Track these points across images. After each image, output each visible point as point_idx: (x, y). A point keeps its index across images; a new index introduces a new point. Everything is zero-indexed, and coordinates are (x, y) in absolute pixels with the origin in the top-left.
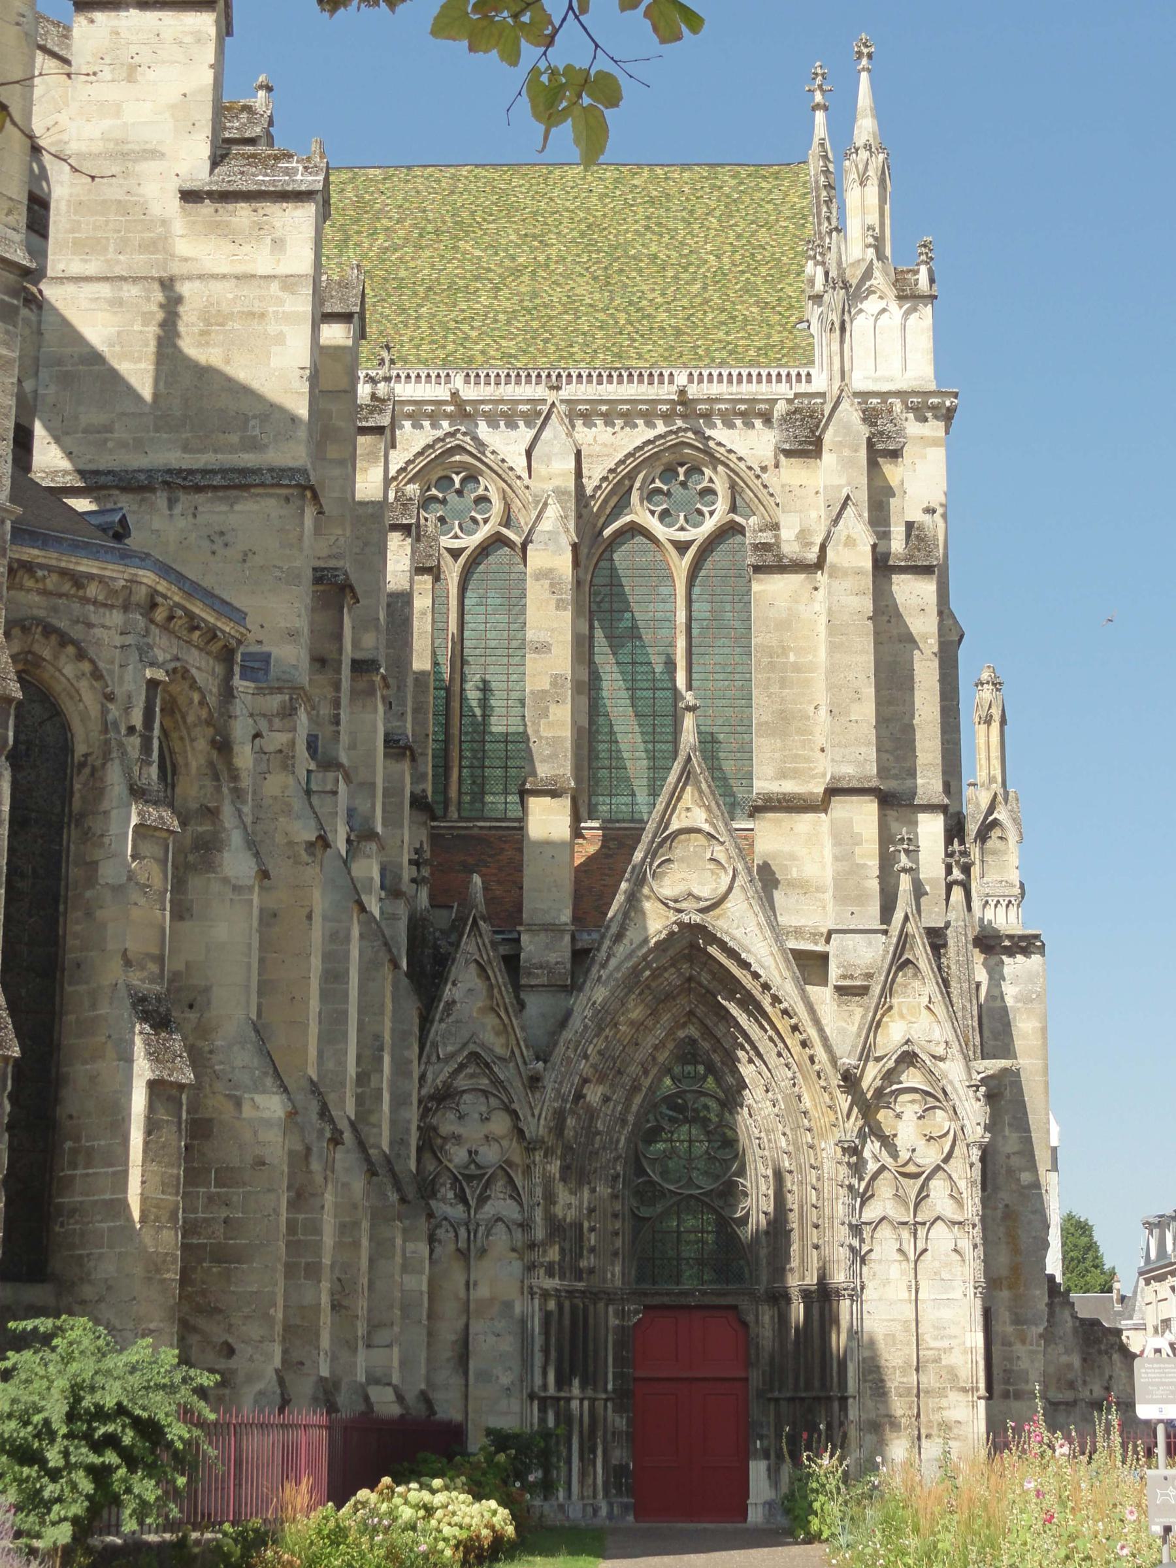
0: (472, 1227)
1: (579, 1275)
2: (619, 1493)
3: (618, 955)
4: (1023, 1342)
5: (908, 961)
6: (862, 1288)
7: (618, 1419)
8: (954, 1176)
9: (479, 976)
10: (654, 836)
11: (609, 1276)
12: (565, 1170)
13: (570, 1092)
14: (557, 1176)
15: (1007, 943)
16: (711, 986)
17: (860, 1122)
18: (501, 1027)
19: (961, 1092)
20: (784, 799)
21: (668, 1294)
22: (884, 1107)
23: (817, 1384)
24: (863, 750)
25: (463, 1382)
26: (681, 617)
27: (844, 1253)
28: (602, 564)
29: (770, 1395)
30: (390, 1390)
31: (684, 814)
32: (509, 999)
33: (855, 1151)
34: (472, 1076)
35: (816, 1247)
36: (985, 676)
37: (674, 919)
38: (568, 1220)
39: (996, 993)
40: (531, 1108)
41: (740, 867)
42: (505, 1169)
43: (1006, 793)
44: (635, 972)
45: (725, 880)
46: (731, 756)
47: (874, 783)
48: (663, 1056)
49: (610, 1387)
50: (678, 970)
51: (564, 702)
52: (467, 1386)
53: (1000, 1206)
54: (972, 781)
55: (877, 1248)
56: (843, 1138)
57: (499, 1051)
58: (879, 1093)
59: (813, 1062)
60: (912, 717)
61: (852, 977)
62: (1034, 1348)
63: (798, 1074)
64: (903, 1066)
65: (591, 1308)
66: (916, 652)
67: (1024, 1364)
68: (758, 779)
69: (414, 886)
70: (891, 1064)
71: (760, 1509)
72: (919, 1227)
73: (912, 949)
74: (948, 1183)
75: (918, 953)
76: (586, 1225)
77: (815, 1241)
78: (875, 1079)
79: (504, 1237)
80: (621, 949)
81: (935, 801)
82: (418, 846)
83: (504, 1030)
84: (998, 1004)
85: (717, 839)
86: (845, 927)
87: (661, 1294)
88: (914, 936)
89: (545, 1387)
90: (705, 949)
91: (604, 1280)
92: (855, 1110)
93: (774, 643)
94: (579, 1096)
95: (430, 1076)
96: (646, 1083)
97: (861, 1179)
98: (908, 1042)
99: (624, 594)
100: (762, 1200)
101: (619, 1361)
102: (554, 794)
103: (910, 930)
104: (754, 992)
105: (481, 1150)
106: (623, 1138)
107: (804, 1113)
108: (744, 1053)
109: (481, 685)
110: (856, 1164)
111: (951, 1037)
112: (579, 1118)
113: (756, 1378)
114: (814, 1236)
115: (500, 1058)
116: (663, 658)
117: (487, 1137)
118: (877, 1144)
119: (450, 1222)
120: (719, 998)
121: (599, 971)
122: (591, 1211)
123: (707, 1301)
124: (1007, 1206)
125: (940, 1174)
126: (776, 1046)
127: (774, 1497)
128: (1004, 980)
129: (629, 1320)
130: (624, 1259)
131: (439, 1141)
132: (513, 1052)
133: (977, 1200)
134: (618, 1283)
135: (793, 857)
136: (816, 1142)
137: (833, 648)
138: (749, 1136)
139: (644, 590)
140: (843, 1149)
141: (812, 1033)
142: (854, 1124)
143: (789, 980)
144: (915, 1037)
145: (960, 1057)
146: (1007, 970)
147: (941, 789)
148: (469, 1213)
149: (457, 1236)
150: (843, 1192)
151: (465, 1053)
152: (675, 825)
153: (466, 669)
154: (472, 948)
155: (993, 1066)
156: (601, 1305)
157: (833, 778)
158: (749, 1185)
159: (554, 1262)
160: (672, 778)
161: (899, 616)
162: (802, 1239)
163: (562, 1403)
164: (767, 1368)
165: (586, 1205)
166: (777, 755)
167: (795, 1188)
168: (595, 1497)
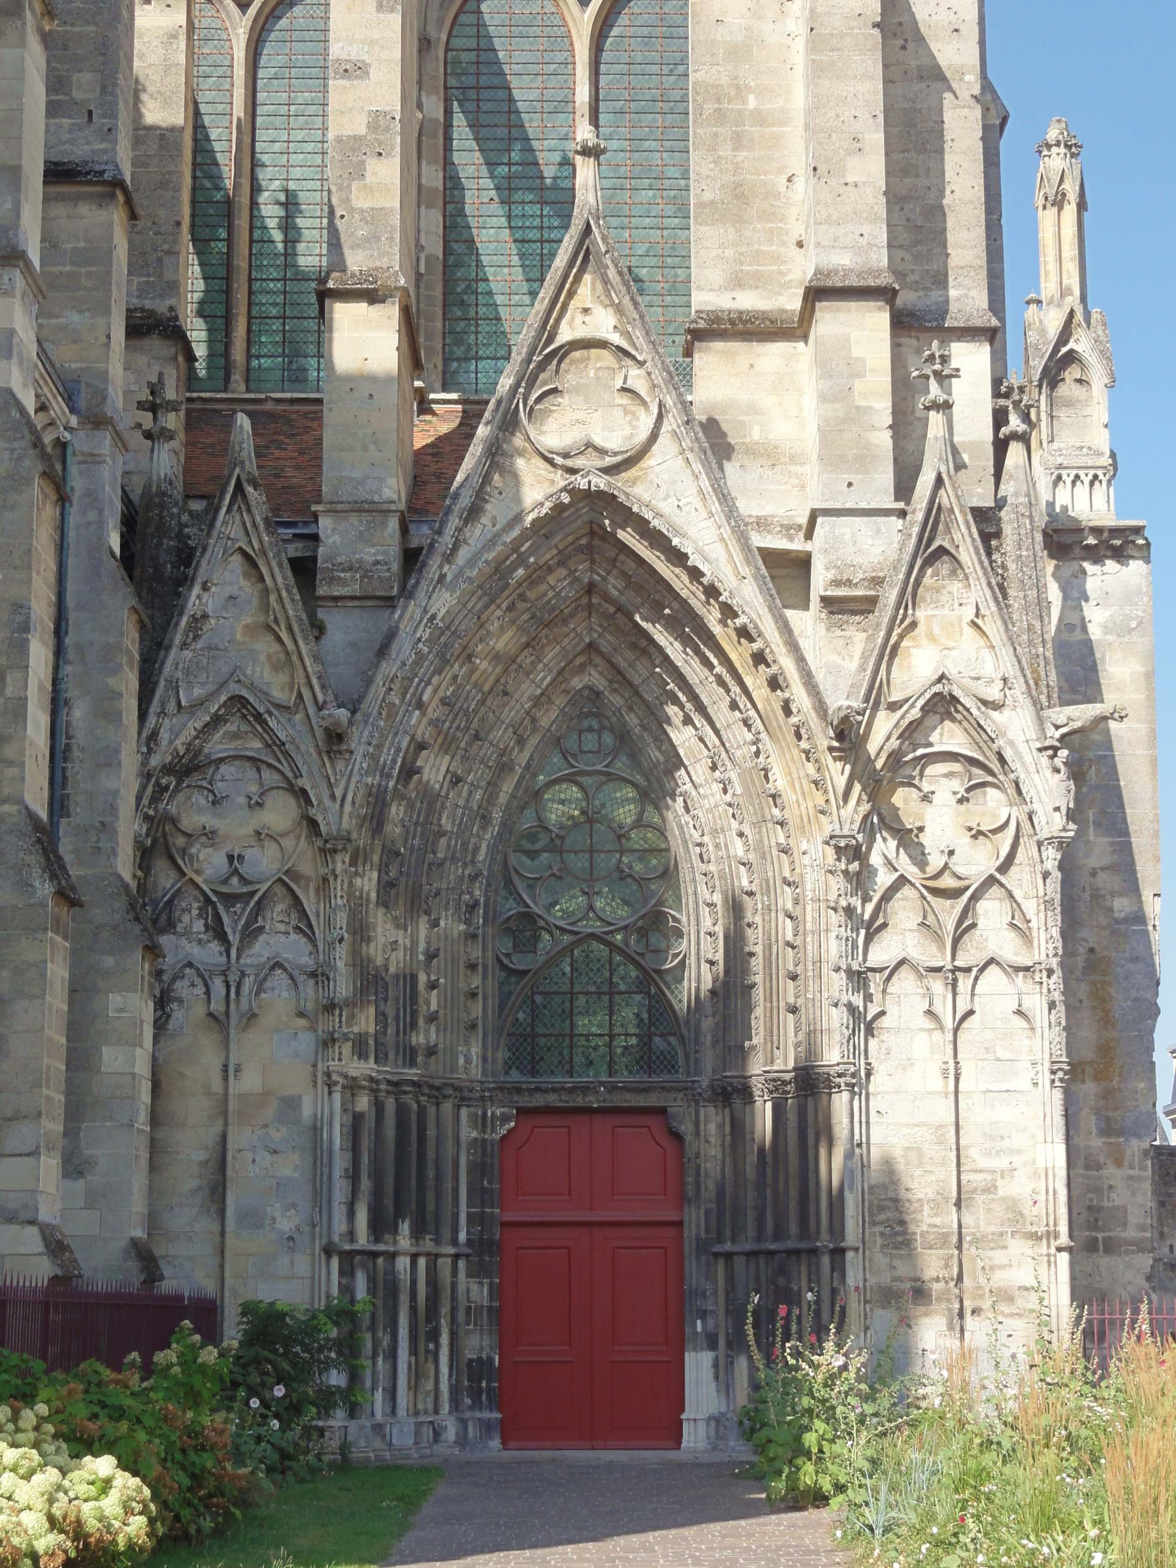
0: (233, 978)
1: (410, 1056)
2: (477, 1404)
4: (1119, 1163)
5: (942, 551)
6: (869, 1074)
7: (474, 1288)
8: (1018, 895)
9: (246, 575)
10: (531, 353)
11: (461, 1061)
12: (387, 887)
13: (394, 761)
14: (373, 895)
15: (1091, 541)
16: (623, 599)
17: (865, 807)
18: (282, 656)
19: (1028, 759)
20: (740, 319)
21: (554, 1090)
22: (903, 784)
23: (793, 1229)
24: (865, 230)
25: (216, 1227)
26: (583, 94)
27: (837, 1018)
28: (464, 18)
29: (717, 1248)
30: (34, 1231)
31: (579, 318)
32: (294, 610)
33: (855, 852)
34: (236, 736)
35: (793, 1010)
36: (1053, 134)
37: (562, 484)
39: (1074, 619)
40: (330, 786)
41: (669, 401)
42: (287, 882)
43: (1087, 316)
44: (500, 571)
45: (646, 422)
46: (657, 300)
47: (885, 280)
49: (462, 1236)
50: (572, 572)
51: (389, 154)
52: (223, 1234)
53: (1081, 950)
54: (1033, 295)
55: (892, 1010)
56: (838, 832)
57: (278, 694)
58: (895, 759)
60: (941, 193)
61: (849, 583)
62: (1135, 1172)
63: (764, 736)
64: (933, 719)
65: (432, 1111)
66: (947, 95)
67: (1119, 1198)
68: (699, 288)
69: (149, 442)
70: (915, 713)
71: (701, 1426)
73: (948, 530)
74: (1007, 906)
75: (957, 537)
76: (422, 978)
77: (792, 1000)
78: (888, 739)
79: (285, 994)
80: (478, 532)
81: (978, 323)
82: (155, 380)
83: (287, 661)
84: (1078, 635)
85: (634, 358)
86: (838, 505)
87: (546, 1091)
88: (952, 510)
89: (351, 1235)
90: (613, 535)
91: (454, 1068)
92: (857, 787)
93: (724, 80)
94: (409, 771)
95: (164, 735)
96: (522, 758)
97: (866, 899)
98: (941, 678)
99: (498, 63)
100: (706, 941)
101: (478, 1194)
102: (372, 297)
104: (693, 602)
105: (249, 854)
107: (774, 797)
108: (676, 709)
109: (282, 198)
110: (858, 874)
111: (1011, 670)
112: (411, 806)
113: (695, 1221)
115: (278, 706)
116: (557, 157)
117: (258, 833)
118: (893, 844)
119: (197, 970)
120: (637, 618)
121: (441, 567)
122: (431, 956)
123: (619, 1100)
124: (1092, 950)
125: (995, 890)
126: (728, 691)
127: (723, 1409)
128: (1087, 600)
129: (493, 1130)
130: (485, 1034)
131: (181, 841)
132: (300, 696)
133: (1055, 932)
134: (476, 1073)
135: (753, 409)
136: (792, 842)
137: (817, 71)
139: (528, 57)
140: (838, 849)
141: (787, 664)
142: (853, 812)
144: (952, 672)
145: (1028, 701)
146: (1091, 585)
147: (985, 305)
148: (228, 956)
149: (208, 993)
150: (835, 918)
151: (223, 698)
152: (565, 335)
153: (262, 175)
154: (235, 530)
155: (1080, 714)
156: (447, 1107)
157: (818, 272)
158: (684, 919)
159: (367, 1033)
160: (560, 261)
161: (921, 39)
162: (769, 997)
163: (380, 1261)
164: (713, 1206)
165: (422, 946)
166: (729, 252)
167: (758, 919)
168: (436, 1411)
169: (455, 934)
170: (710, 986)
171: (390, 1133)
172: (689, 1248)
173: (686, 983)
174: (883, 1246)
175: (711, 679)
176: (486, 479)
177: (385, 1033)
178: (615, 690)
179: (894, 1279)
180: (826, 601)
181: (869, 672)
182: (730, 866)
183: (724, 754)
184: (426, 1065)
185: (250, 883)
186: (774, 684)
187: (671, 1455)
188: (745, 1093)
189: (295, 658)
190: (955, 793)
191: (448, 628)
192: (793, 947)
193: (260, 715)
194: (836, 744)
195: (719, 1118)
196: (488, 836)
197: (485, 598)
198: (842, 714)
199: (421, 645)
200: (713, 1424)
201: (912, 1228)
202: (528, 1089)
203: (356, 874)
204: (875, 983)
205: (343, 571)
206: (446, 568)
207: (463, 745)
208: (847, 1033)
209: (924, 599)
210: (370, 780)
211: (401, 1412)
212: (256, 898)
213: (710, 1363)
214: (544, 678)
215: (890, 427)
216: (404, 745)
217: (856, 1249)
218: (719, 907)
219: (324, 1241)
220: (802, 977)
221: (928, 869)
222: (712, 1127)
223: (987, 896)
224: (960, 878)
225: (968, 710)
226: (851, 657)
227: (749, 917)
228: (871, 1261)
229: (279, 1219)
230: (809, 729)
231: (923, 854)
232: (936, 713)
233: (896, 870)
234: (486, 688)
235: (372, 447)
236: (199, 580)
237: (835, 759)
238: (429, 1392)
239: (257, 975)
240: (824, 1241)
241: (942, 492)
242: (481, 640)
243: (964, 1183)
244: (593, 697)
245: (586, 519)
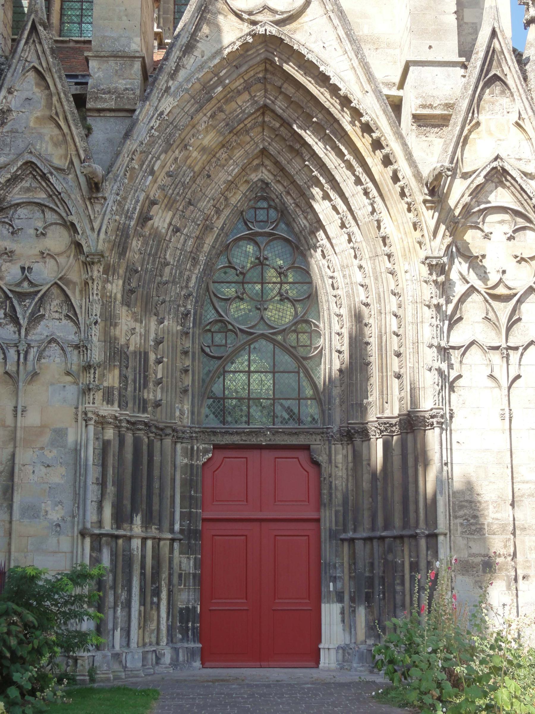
0: (22, 347)
2: (185, 637)
3: (188, 67)
5: (496, 78)
6: (451, 417)
7: (185, 561)
9: (38, 85)
11: (177, 413)
13: (135, 209)
14: (119, 296)
16: (285, 115)
17: (448, 240)
18: (61, 138)
21: (237, 433)
22: (472, 227)
23: (397, 521)
25: (6, 517)
29: (343, 536)
34: (28, 190)
35: (398, 376)
37: (247, 31)
38: (132, 348)
40: (91, 221)
48: (235, 198)
49: (177, 527)
50: (252, 98)
52: (11, 522)
57: (57, 162)
59: (379, 227)
61: (431, 106)
63: (378, 199)
64: (490, 186)
65: (157, 444)
70: (480, 180)
71: (333, 653)
72: (511, 352)
75: (506, 69)
76: (152, 357)
77: (397, 370)
78: (463, 196)
79: (58, 360)
80: (192, 60)
87: (232, 434)
89: (100, 524)
90: (281, 67)
91: (172, 416)
92: (443, 227)
96: (219, 224)
97: (448, 301)
98: (497, 158)
103: (497, 46)
104: (332, 110)
105: (35, 267)
106: (194, 277)
107: (384, 239)
108: (317, 190)
110: (443, 284)
112: (145, 243)
114: (395, 364)
115: (57, 169)
120: (295, 127)
121: (167, 82)
122: (158, 342)
123: (280, 440)
127: (348, 642)
132: (72, 162)
134: (187, 421)
136: (396, 267)
138: (322, 277)
140: (431, 266)
143: (371, 94)
148: (20, 334)
149: (5, 358)
150: (428, 313)
151: (20, 163)
154: (32, 57)
156: (168, 441)
158: (321, 325)
163: (120, 541)
164: (341, 508)
165: (152, 336)
167: (371, 321)
168: (158, 643)
169: (175, 330)
170: (338, 367)
171: (129, 456)
172: (324, 535)
173: (322, 366)
174: (462, 533)
175: (343, 165)
176: (198, 28)
177: (126, 389)
178: (279, 181)
179: (470, 555)
180: (417, 118)
181: (450, 152)
182: (352, 289)
183: (350, 217)
184: (154, 413)
185: (36, 286)
186: (387, 161)
187: (313, 673)
188: (365, 434)
189: (69, 138)
190: (505, 234)
191: (172, 123)
192: (398, 336)
193: (45, 174)
194: (428, 198)
195: (345, 452)
196: (196, 271)
197: (196, 106)
198: (436, 172)
199: (153, 131)
200: (341, 651)
201: (482, 520)
202: (220, 432)
203: (107, 281)
204: (455, 355)
205: (104, 93)
206: (171, 83)
207: (181, 208)
208: (438, 388)
209: (484, 108)
210: (117, 217)
211: (133, 645)
212: (39, 295)
213: (339, 611)
214: (233, 170)
215: (455, 13)
216: (141, 198)
217: (445, 535)
218: (344, 317)
219: (81, 527)
220: (404, 355)
221: (489, 283)
222: (340, 458)
223: (528, 300)
224: (510, 289)
225: (514, 179)
226: (432, 154)
227: (366, 321)
228: (454, 542)
229: (50, 512)
230: (411, 189)
231: (485, 273)
232: (492, 182)
233: (468, 282)
234: (196, 169)
235: (124, 18)
236: (6, 86)
237: (428, 208)
238: (152, 632)
239: (39, 347)
240: (422, 529)
241: (495, 41)
242: (193, 136)
243: (516, 490)
244: (264, 186)
245: (263, 56)
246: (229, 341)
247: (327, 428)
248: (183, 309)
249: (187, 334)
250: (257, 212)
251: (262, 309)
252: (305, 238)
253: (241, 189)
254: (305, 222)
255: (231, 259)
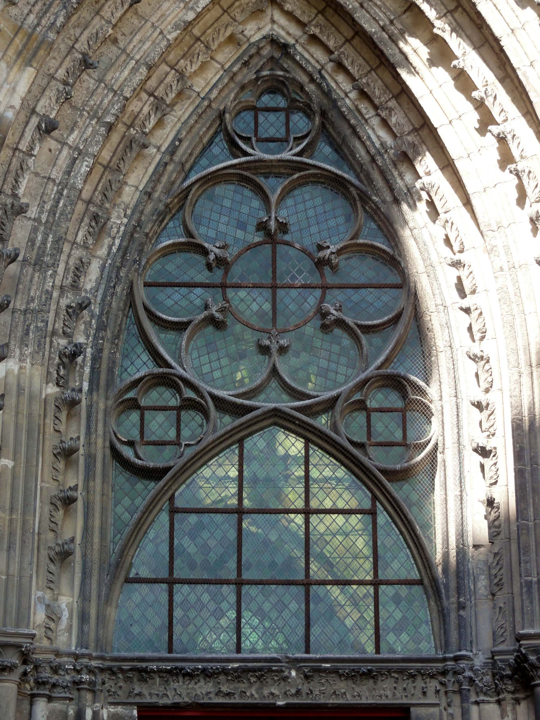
21: (207, 674)
87: (190, 676)
178: (314, 38)
196: (102, 252)
202: (160, 671)
207: (61, 73)
246: (185, 433)
247: (456, 659)
248: (63, 342)
249: (73, 403)
250: (261, 119)
251: (274, 348)
252: (382, 173)
253: (220, 57)
254: (383, 134)
255: (192, 227)
